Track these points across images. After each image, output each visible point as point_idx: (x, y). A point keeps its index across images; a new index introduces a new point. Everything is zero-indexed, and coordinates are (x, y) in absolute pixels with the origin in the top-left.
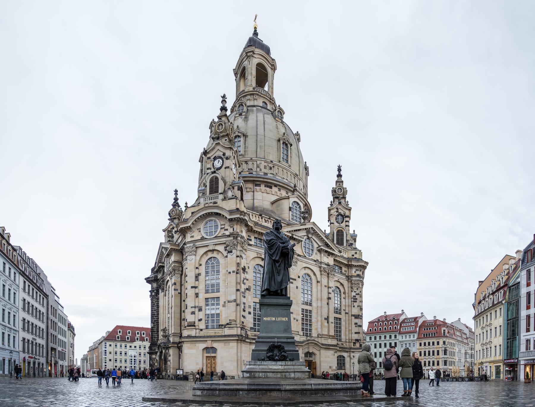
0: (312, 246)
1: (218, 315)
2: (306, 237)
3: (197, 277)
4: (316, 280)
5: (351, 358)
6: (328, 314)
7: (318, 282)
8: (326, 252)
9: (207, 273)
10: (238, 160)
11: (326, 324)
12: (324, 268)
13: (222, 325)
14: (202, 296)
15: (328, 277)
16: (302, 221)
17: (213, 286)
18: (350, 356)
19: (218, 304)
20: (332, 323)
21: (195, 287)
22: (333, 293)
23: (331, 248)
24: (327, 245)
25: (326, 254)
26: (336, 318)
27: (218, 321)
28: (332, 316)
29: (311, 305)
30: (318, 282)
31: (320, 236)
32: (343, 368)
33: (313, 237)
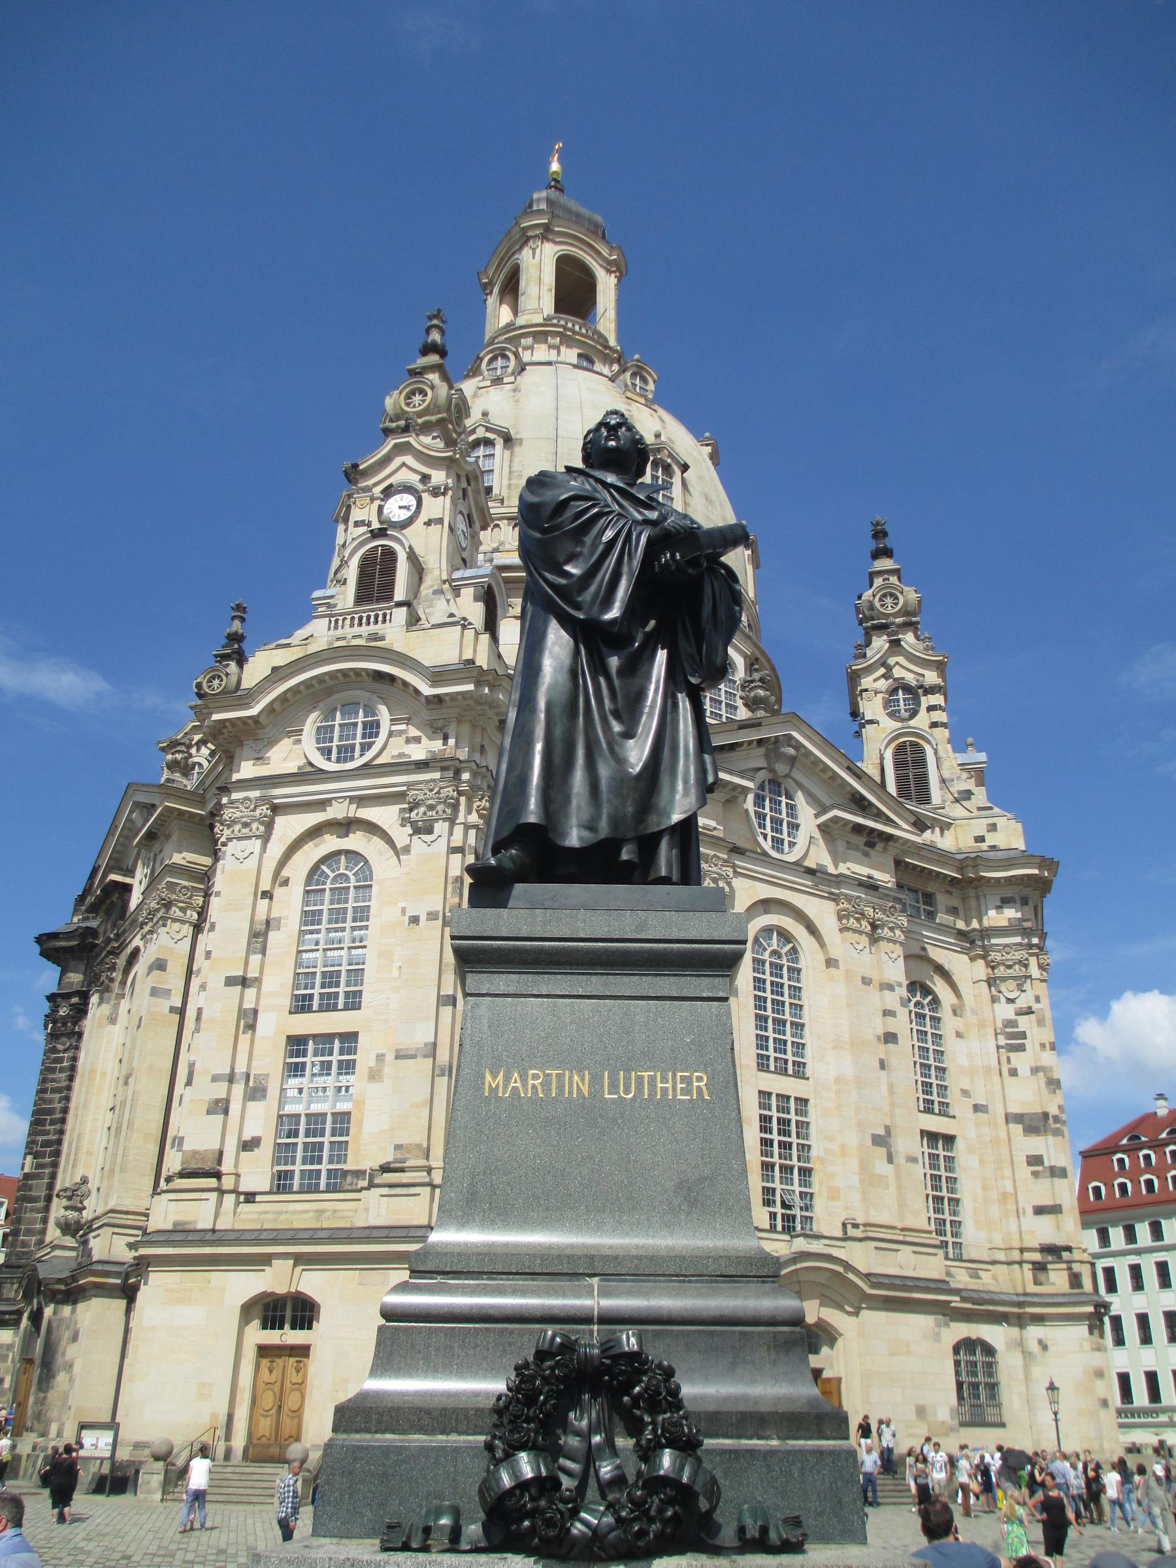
0: (791, 808)
1: (343, 1120)
2: (762, 775)
3: (259, 936)
4: (821, 957)
5: (1027, 1355)
6: (892, 1115)
7: (831, 963)
8: (858, 829)
9: (310, 918)
10: (476, 503)
11: (883, 1168)
12: (849, 899)
13: (359, 1174)
14: (276, 1023)
15: (874, 940)
16: (743, 714)
17: (331, 979)
18: (1021, 1344)
19: (347, 1067)
20: (912, 1160)
21: (244, 982)
22: (903, 1013)
23: (879, 816)
24: (859, 803)
25: (860, 840)
26: (931, 1137)
27: (340, 1149)
28: (911, 1123)
29: (800, 1071)
30: (831, 963)
31: (827, 768)
32: (990, 1414)
33: (796, 774)
